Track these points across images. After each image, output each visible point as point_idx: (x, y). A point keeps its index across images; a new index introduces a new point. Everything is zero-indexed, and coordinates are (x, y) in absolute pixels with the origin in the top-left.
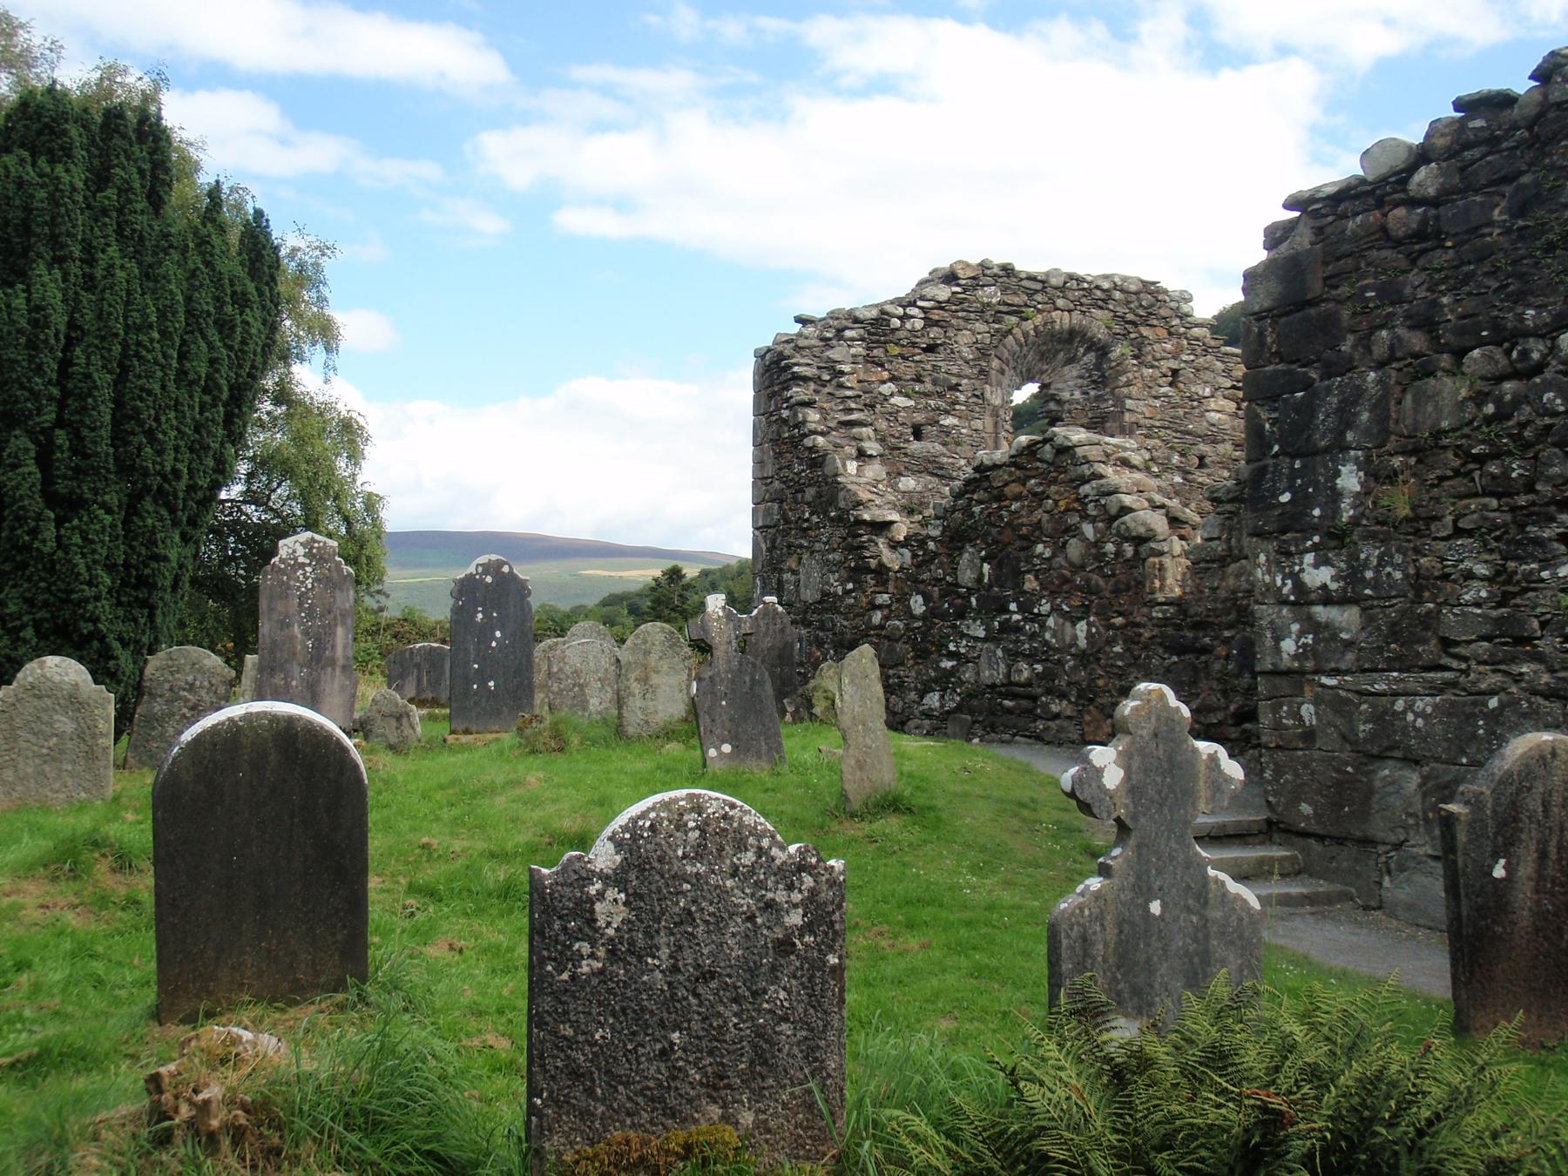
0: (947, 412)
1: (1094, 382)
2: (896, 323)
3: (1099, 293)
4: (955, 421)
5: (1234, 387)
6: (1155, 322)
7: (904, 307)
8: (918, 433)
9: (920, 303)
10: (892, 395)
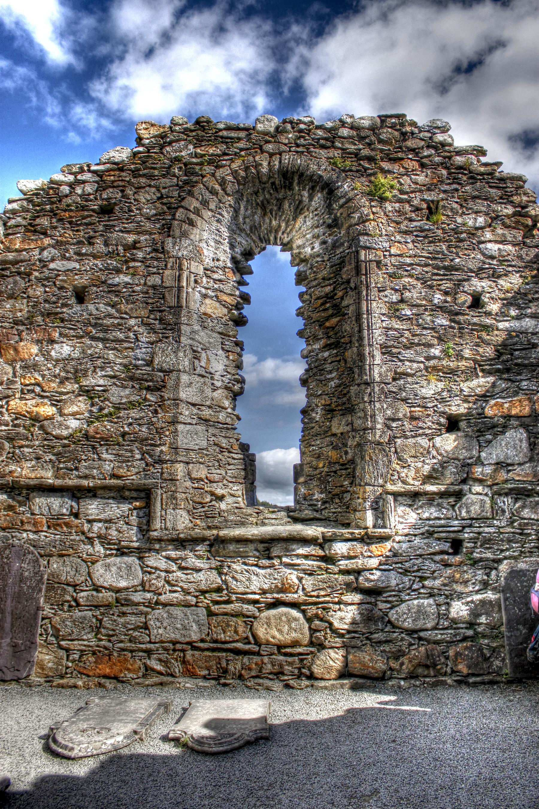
0: (118, 271)
1: (329, 226)
2: (66, 189)
3: (320, 133)
4: (127, 279)
5: (515, 214)
6: (400, 155)
7: (75, 174)
8: (81, 296)
9: (93, 168)
10: (53, 260)
